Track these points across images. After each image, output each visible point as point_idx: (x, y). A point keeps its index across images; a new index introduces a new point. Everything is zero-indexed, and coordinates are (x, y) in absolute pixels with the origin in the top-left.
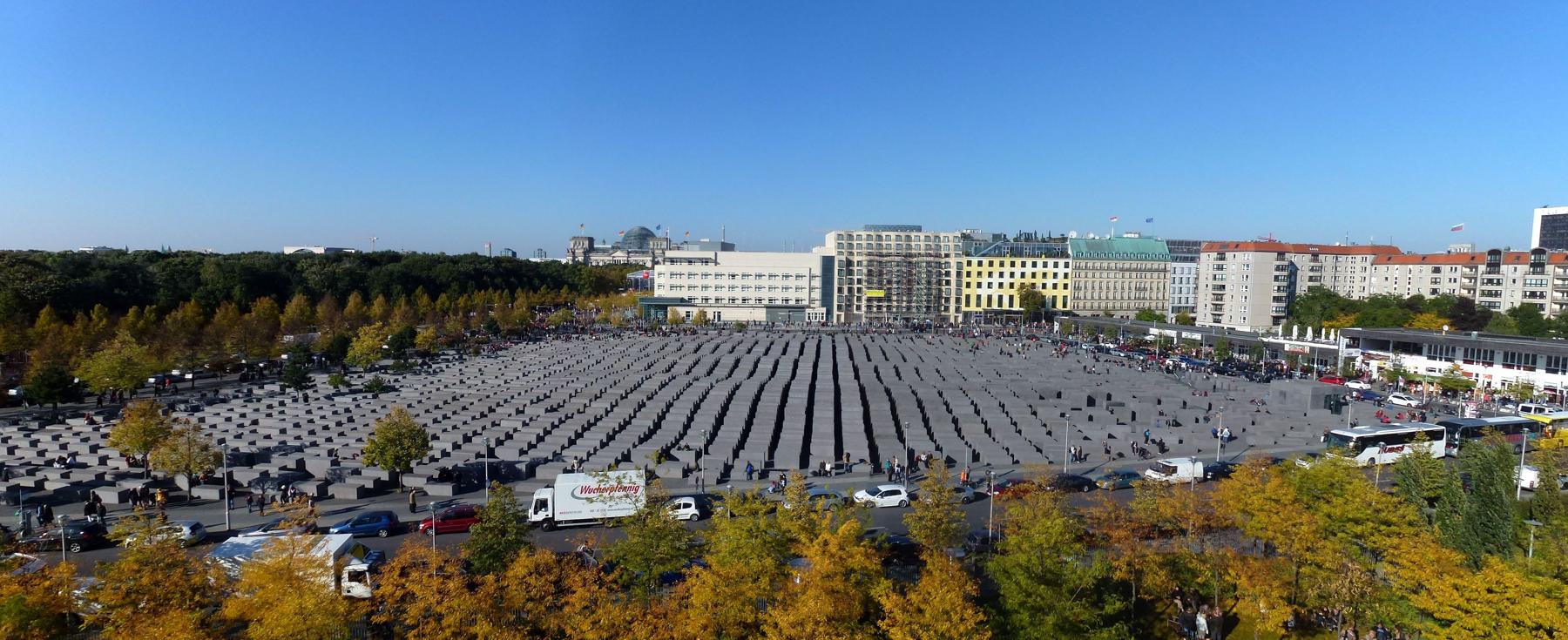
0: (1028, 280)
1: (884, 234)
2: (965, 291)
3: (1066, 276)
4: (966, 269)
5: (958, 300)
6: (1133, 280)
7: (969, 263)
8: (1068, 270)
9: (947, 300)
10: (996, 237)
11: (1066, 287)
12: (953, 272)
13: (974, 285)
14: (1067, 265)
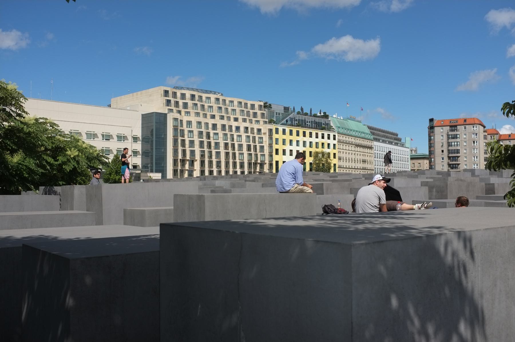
0: (314, 150)
1: (204, 96)
2: (276, 158)
3: (334, 145)
4: (275, 136)
5: (271, 165)
6: (360, 154)
7: (277, 132)
8: (335, 142)
9: (262, 165)
10: (286, 109)
11: (335, 154)
12: (266, 138)
13: (281, 152)
14: (334, 139)
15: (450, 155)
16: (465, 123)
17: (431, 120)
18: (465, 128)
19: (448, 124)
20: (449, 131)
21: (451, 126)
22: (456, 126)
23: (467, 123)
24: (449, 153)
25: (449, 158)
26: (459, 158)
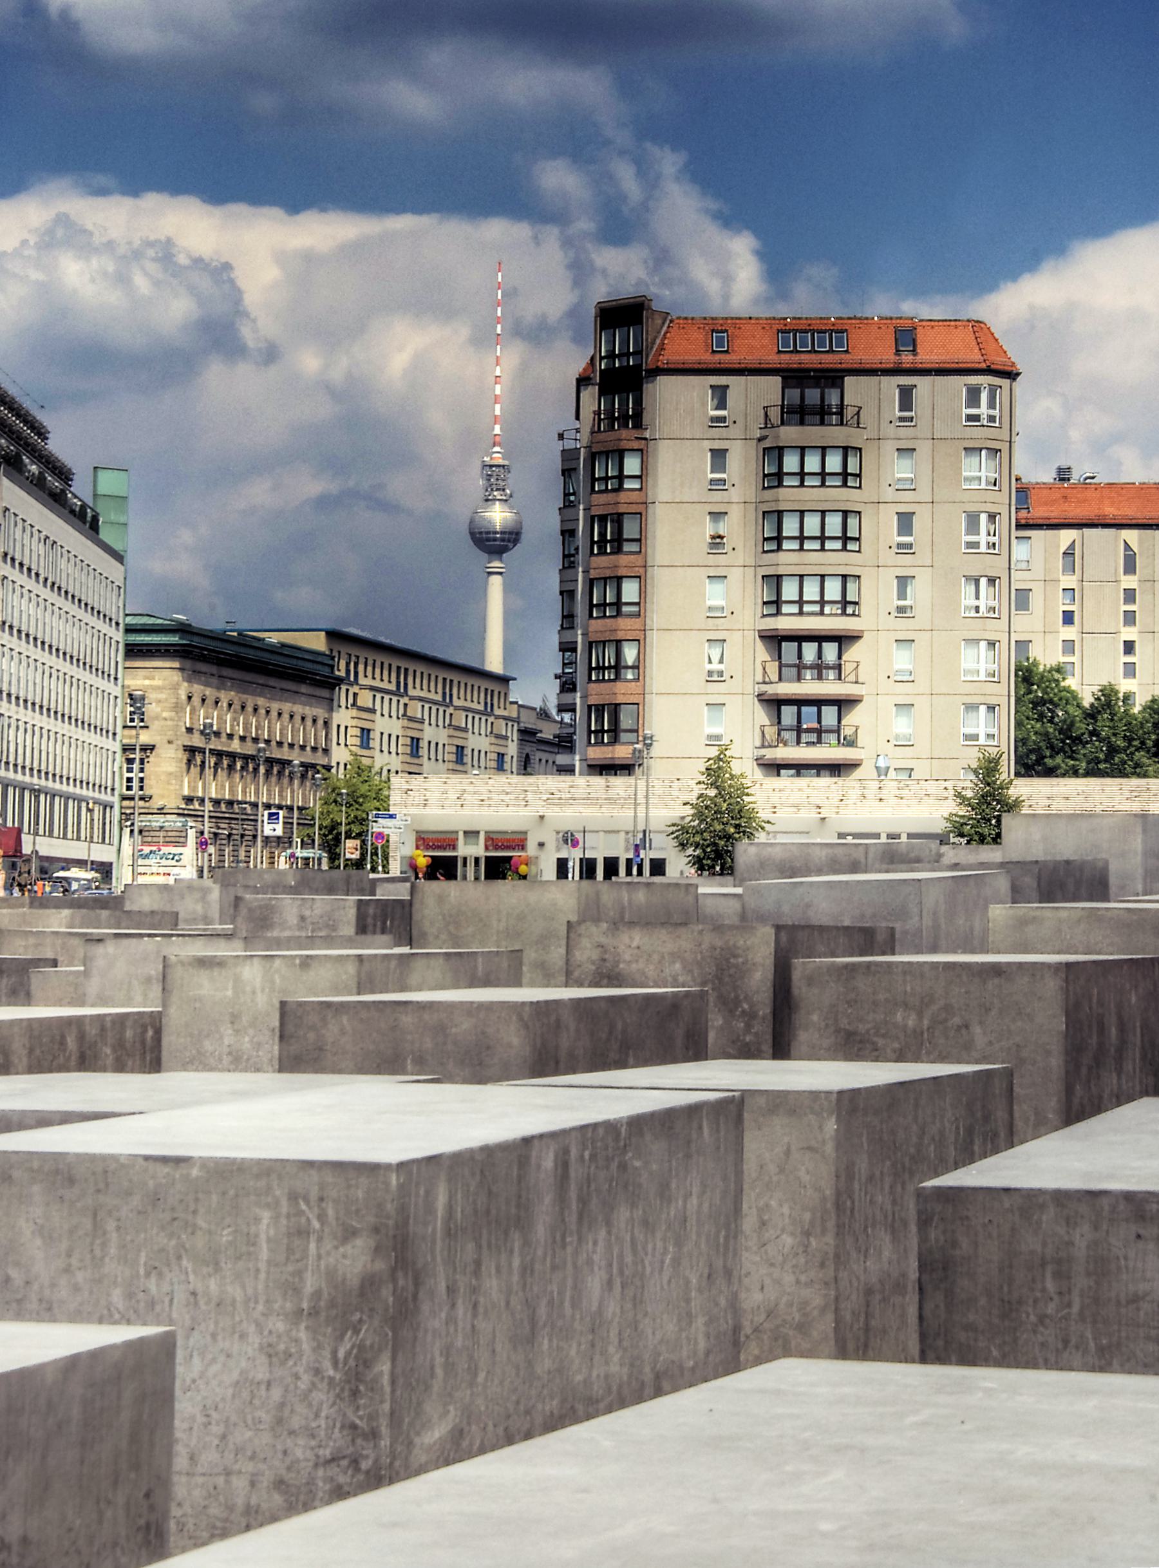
15: (786, 623)
16: (907, 359)
17: (622, 316)
18: (906, 396)
19: (763, 349)
20: (775, 415)
21: (793, 377)
22: (834, 378)
23: (927, 355)
24: (776, 604)
25: (775, 640)
26: (853, 653)
